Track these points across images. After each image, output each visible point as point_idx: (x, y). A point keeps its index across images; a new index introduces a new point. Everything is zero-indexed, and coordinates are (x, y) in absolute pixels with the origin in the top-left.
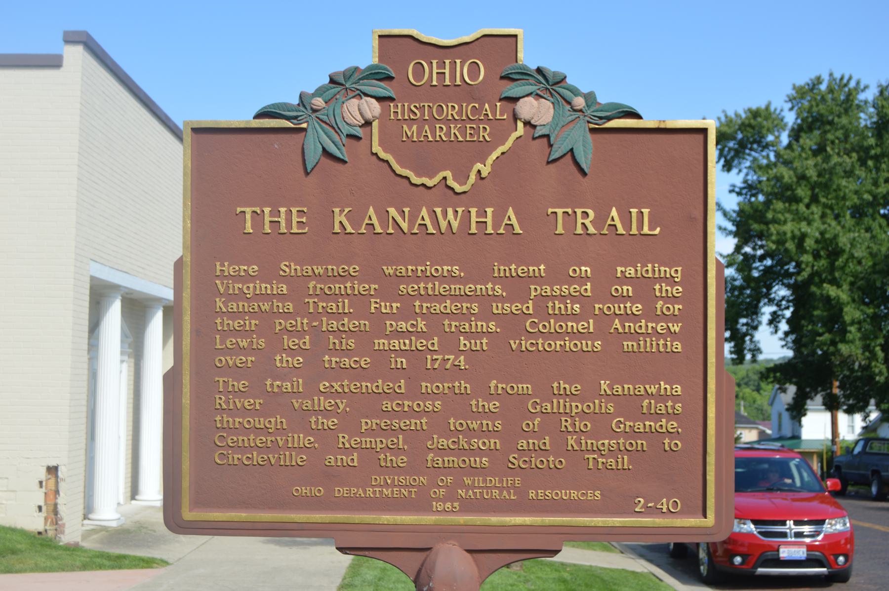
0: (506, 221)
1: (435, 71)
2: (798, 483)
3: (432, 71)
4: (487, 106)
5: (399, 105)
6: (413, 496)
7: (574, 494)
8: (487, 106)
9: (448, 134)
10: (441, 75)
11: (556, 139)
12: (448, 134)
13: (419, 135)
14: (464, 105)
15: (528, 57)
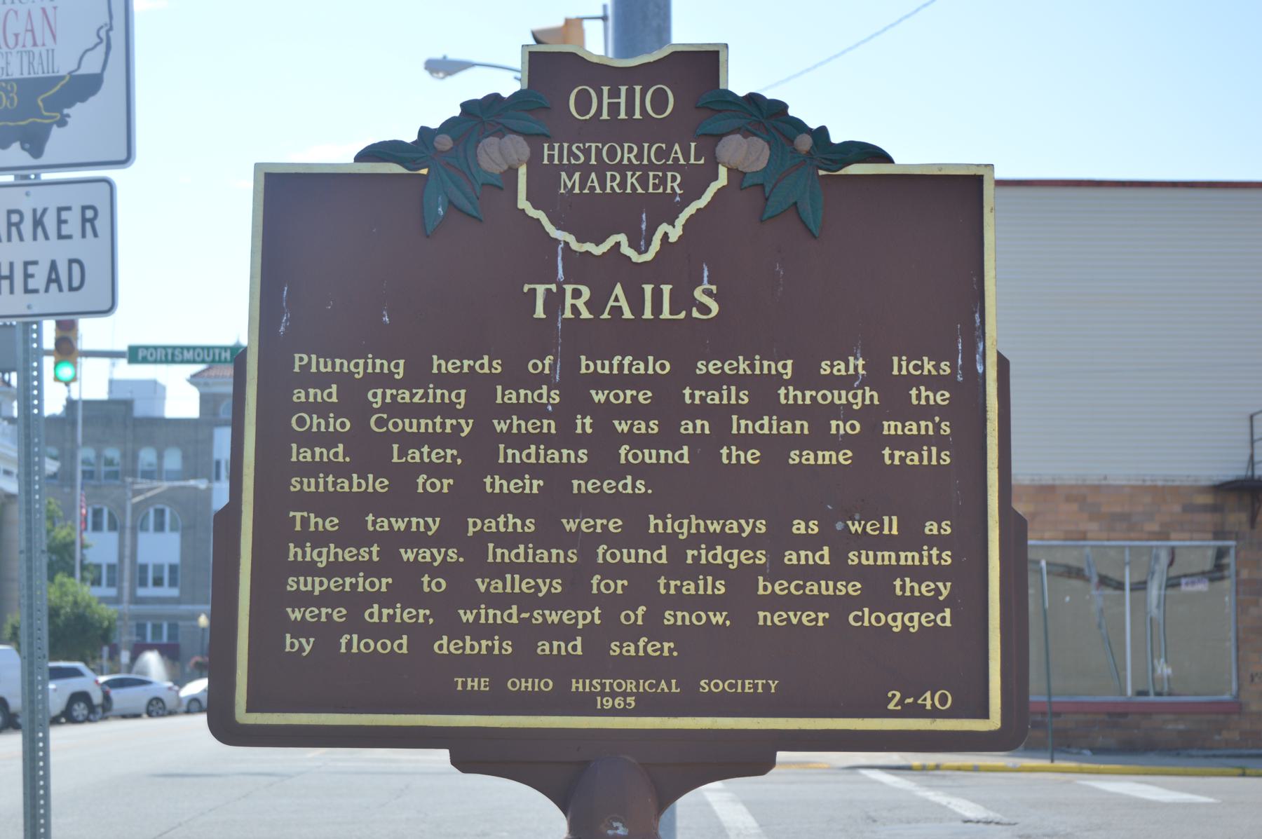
0: (611, 303)
1: (606, 101)
2: (929, 707)
3: (601, 103)
4: (677, 147)
5: (557, 145)
6: (760, 690)
7: (723, 686)
8: (677, 147)
9: (623, 185)
10: (614, 108)
11: (771, 192)
12: (623, 185)
13: (582, 187)
14: (646, 145)
15: (740, 80)
